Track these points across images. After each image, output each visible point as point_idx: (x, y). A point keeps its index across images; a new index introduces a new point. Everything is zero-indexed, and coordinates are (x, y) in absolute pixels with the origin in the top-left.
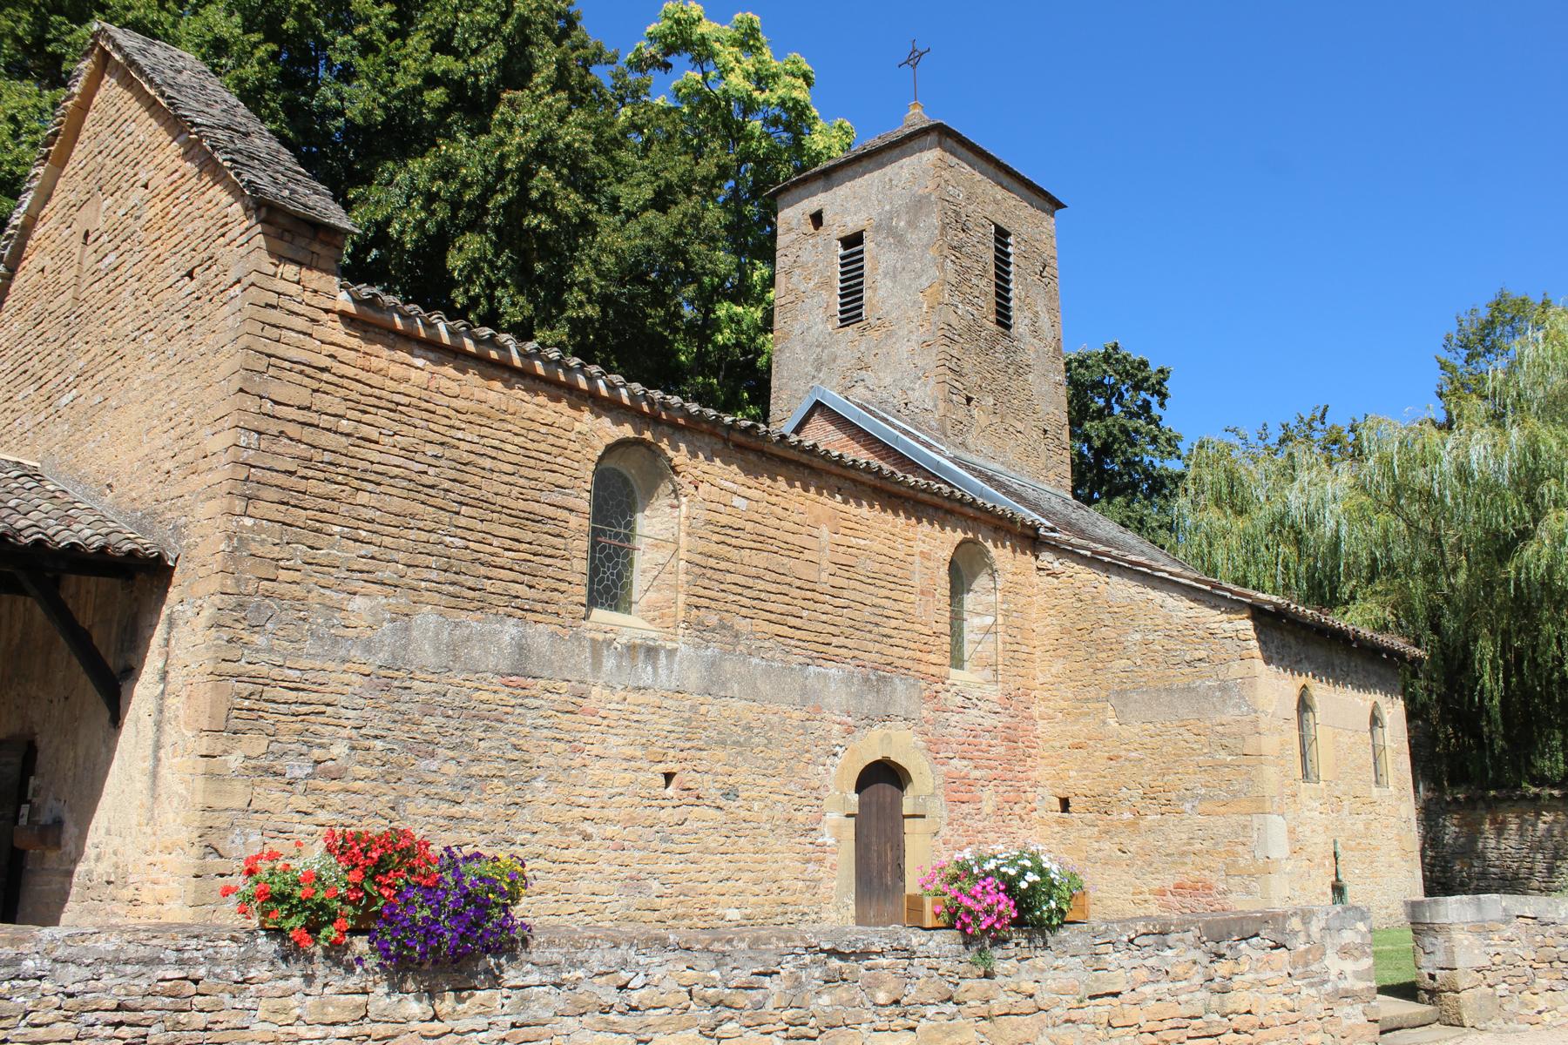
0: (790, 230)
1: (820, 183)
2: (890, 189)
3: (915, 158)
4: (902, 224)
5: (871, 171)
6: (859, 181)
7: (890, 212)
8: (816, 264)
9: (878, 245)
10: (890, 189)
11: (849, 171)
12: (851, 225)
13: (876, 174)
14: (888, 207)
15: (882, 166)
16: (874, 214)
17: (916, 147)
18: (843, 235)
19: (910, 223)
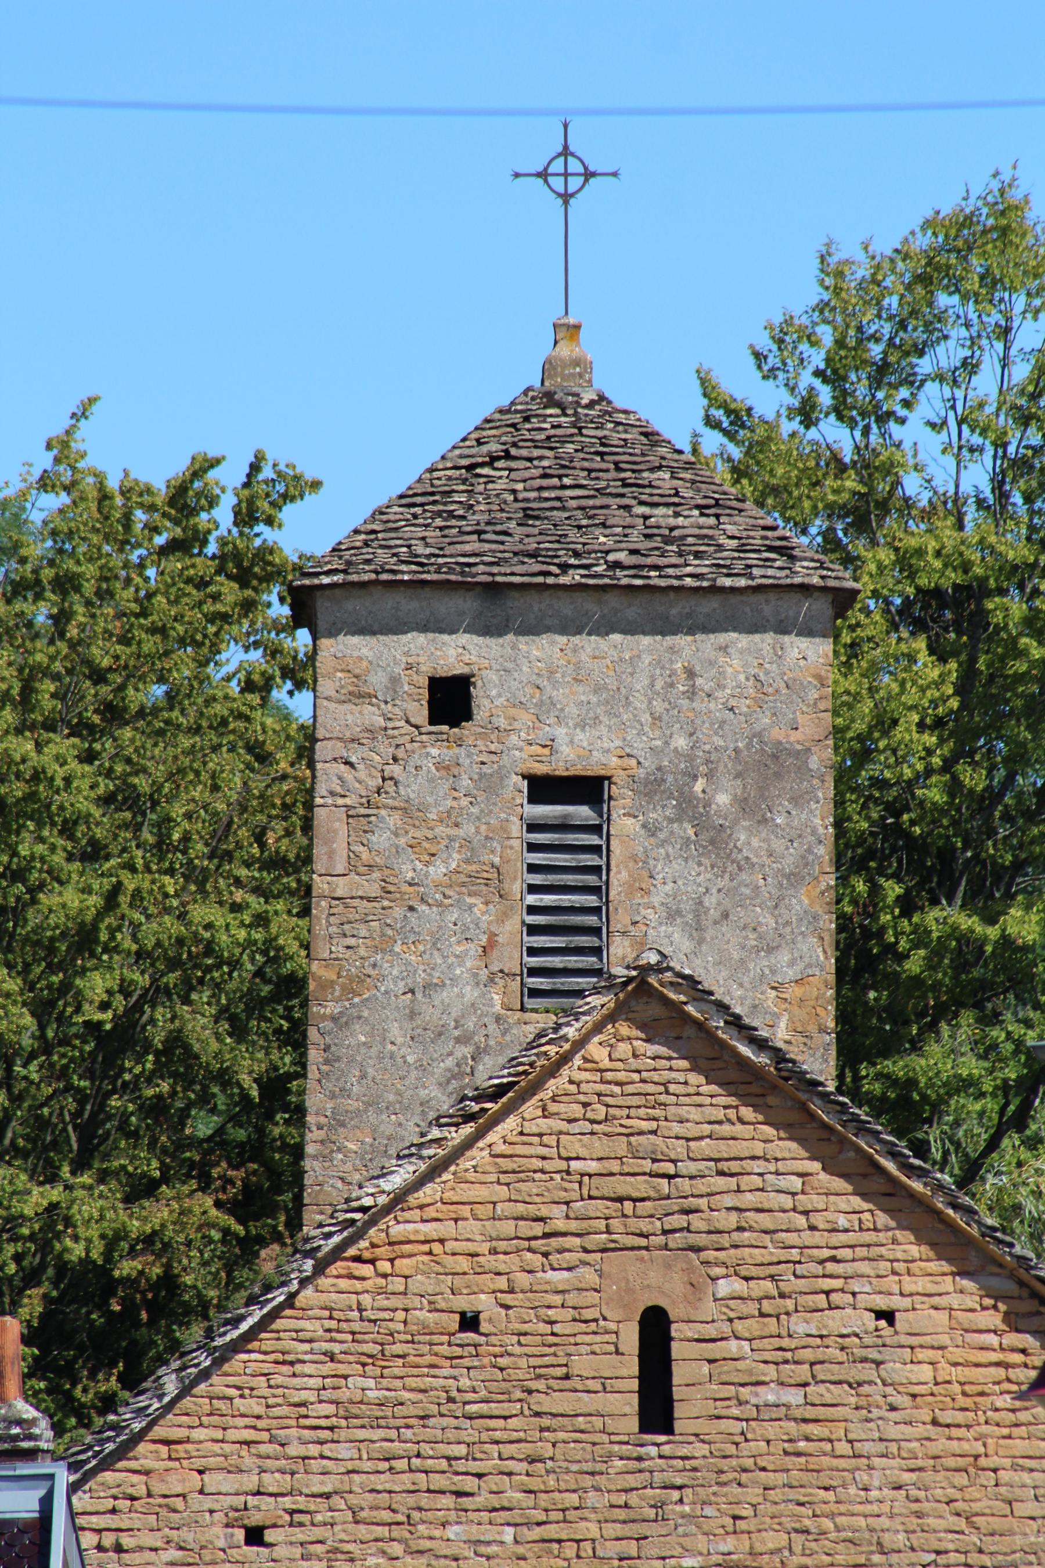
0: (360, 696)
1: (468, 604)
2: (692, 694)
3: (765, 640)
4: (723, 799)
5: (630, 629)
6: (588, 644)
7: (690, 758)
8: (450, 818)
9: (651, 830)
10: (692, 694)
11: (565, 606)
12: (566, 751)
13: (646, 640)
14: (681, 742)
15: (665, 627)
16: (639, 747)
17: (767, 610)
18: (541, 769)
19: (743, 804)
